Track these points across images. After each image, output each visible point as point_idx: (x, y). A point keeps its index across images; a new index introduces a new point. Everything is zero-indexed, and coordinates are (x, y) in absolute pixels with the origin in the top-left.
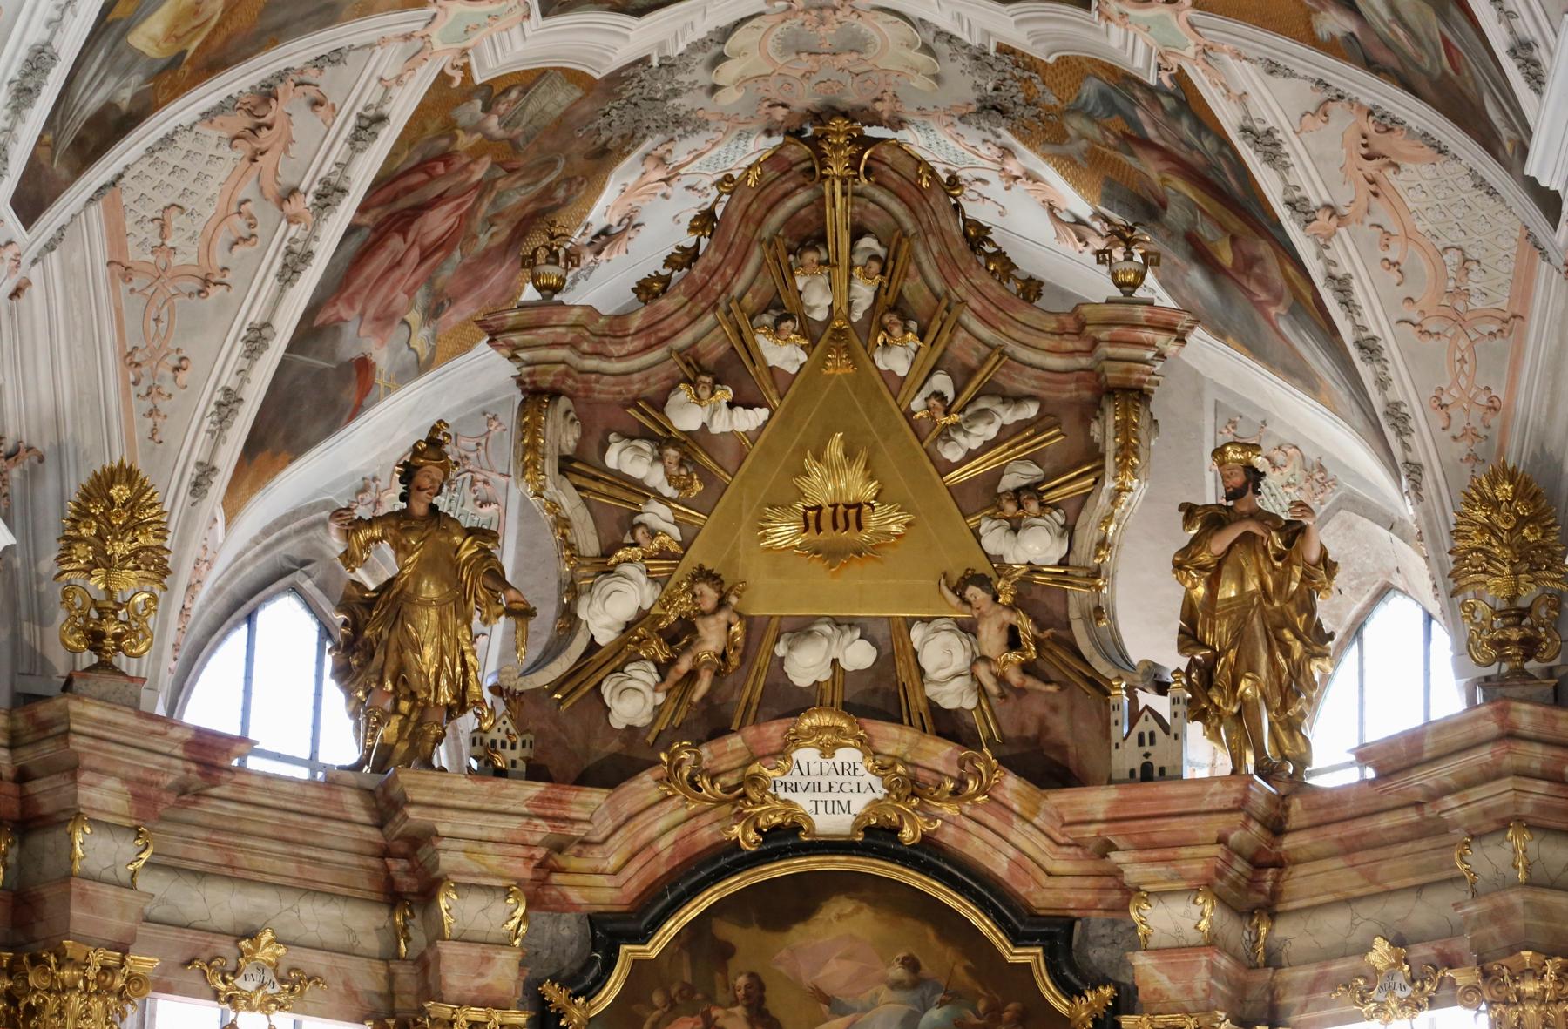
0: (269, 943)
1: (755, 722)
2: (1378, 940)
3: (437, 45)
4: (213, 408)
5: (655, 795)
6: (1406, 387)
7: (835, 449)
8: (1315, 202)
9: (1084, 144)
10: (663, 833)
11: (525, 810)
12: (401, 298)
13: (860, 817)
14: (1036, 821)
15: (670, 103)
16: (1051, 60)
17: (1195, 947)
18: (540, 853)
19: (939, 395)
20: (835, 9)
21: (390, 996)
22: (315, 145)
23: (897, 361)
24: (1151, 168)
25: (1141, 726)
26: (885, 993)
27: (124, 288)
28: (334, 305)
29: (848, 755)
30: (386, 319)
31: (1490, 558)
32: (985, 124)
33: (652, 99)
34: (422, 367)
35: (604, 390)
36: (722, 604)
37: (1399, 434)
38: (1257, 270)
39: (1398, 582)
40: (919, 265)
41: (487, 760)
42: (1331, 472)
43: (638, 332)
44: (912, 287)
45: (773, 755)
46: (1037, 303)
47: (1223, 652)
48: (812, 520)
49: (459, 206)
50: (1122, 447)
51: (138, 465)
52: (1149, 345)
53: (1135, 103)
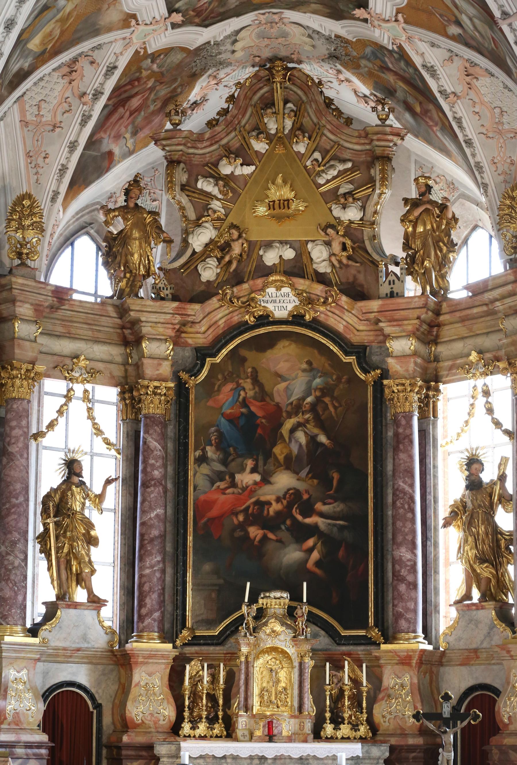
0: (83, 360)
1: (253, 279)
2: (473, 352)
3: (135, 41)
4: (58, 171)
5: (217, 305)
6: (482, 157)
7: (279, 180)
8: (449, 91)
9: (366, 69)
10: (221, 318)
11: (172, 312)
12: (123, 129)
13: (290, 312)
14: (353, 312)
15: (218, 57)
16: (354, 40)
17: (409, 356)
18: (177, 327)
19: (316, 160)
20: (277, 23)
21: (126, 377)
22: (92, 77)
23: (301, 148)
24: (391, 78)
25: (390, 278)
26: (300, 373)
27: (26, 130)
28: (99, 133)
29: (286, 290)
30: (118, 137)
31: (512, 217)
33: (211, 56)
34: (131, 153)
35: (196, 160)
36: (240, 236)
37: (480, 173)
38: (429, 114)
39: (480, 224)
40: (308, 113)
41: (157, 294)
42: (456, 185)
43: (208, 139)
44: (306, 121)
45: (259, 290)
46: (351, 126)
47: (419, 251)
48: (271, 206)
49: (143, 96)
50: (382, 178)
51: (32, 193)
52: (391, 141)
53: (384, 55)
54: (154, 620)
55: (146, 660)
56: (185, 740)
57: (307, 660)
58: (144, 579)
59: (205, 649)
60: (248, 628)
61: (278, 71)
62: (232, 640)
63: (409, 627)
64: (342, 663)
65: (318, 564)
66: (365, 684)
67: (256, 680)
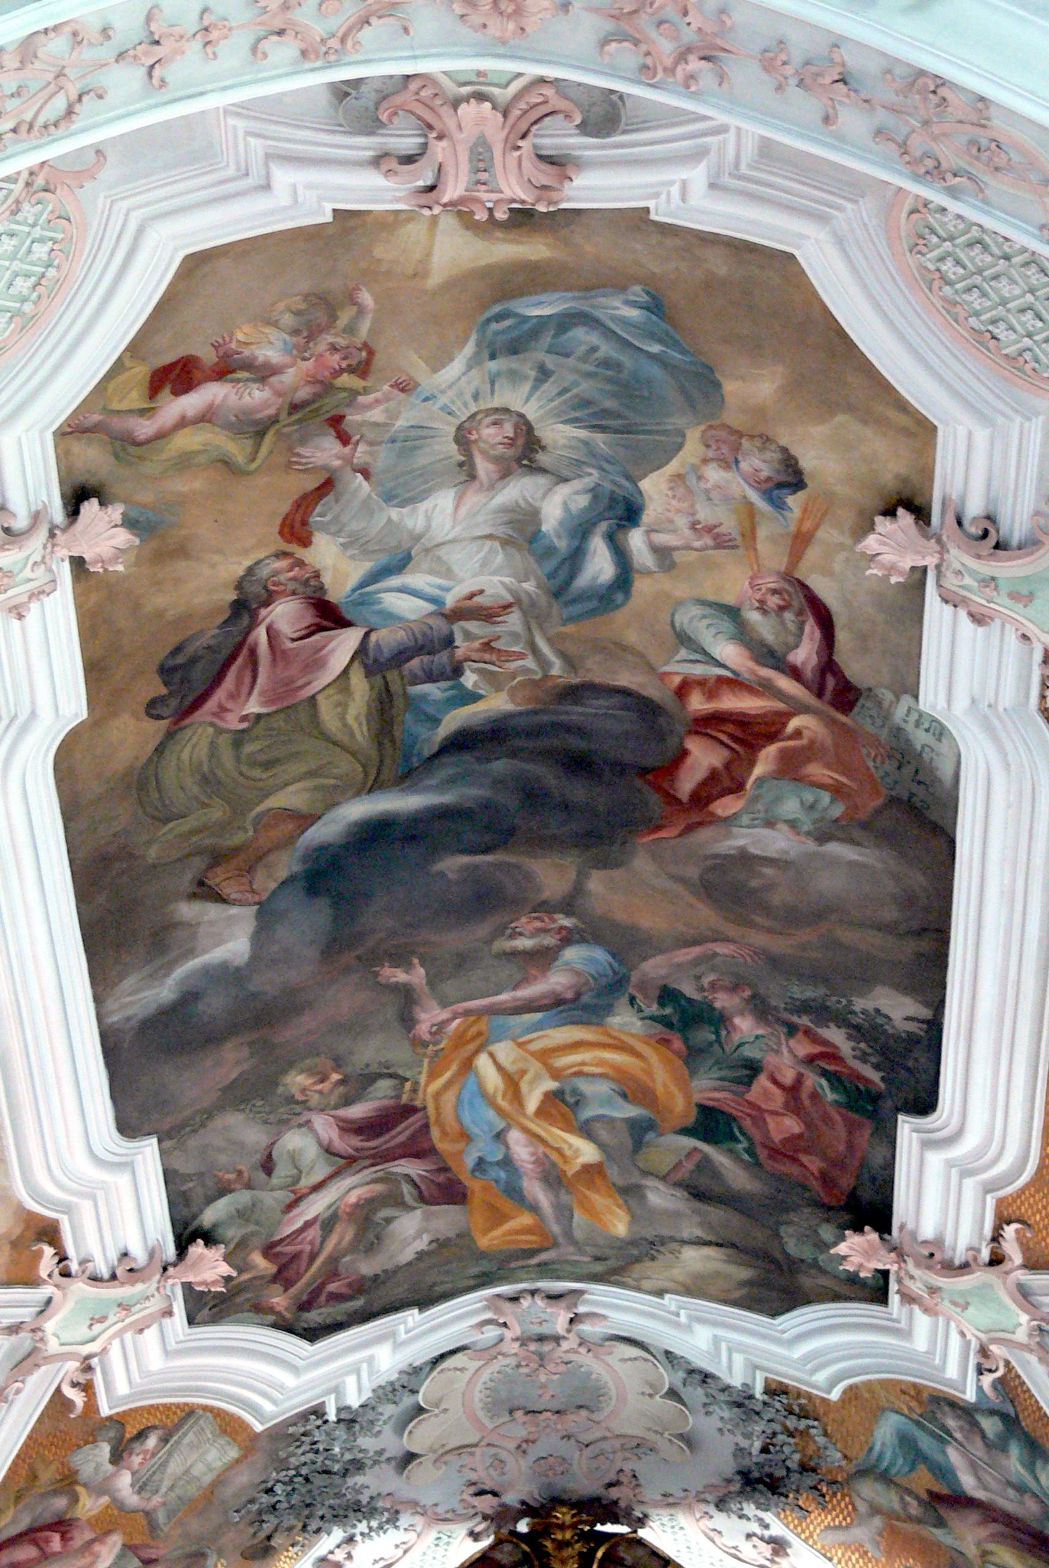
15: (350, 1481)
32: (750, 1509)
33: (327, 1472)
53: (944, 1437)
61: (562, 1545)
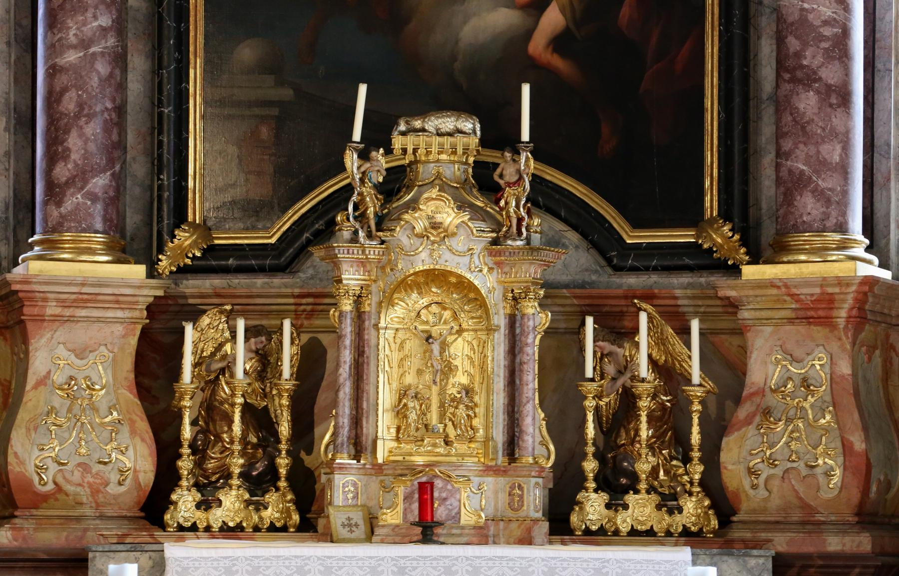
54: (94, 198)
55: (68, 312)
56: (182, 539)
57: (530, 308)
58: (62, 80)
59: (240, 282)
60: (361, 217)
62: (318, 252)
63: (826, 216)
64: (627, 323)
65: (559, 43)
66: (696, 377)
67: (384, 364)
